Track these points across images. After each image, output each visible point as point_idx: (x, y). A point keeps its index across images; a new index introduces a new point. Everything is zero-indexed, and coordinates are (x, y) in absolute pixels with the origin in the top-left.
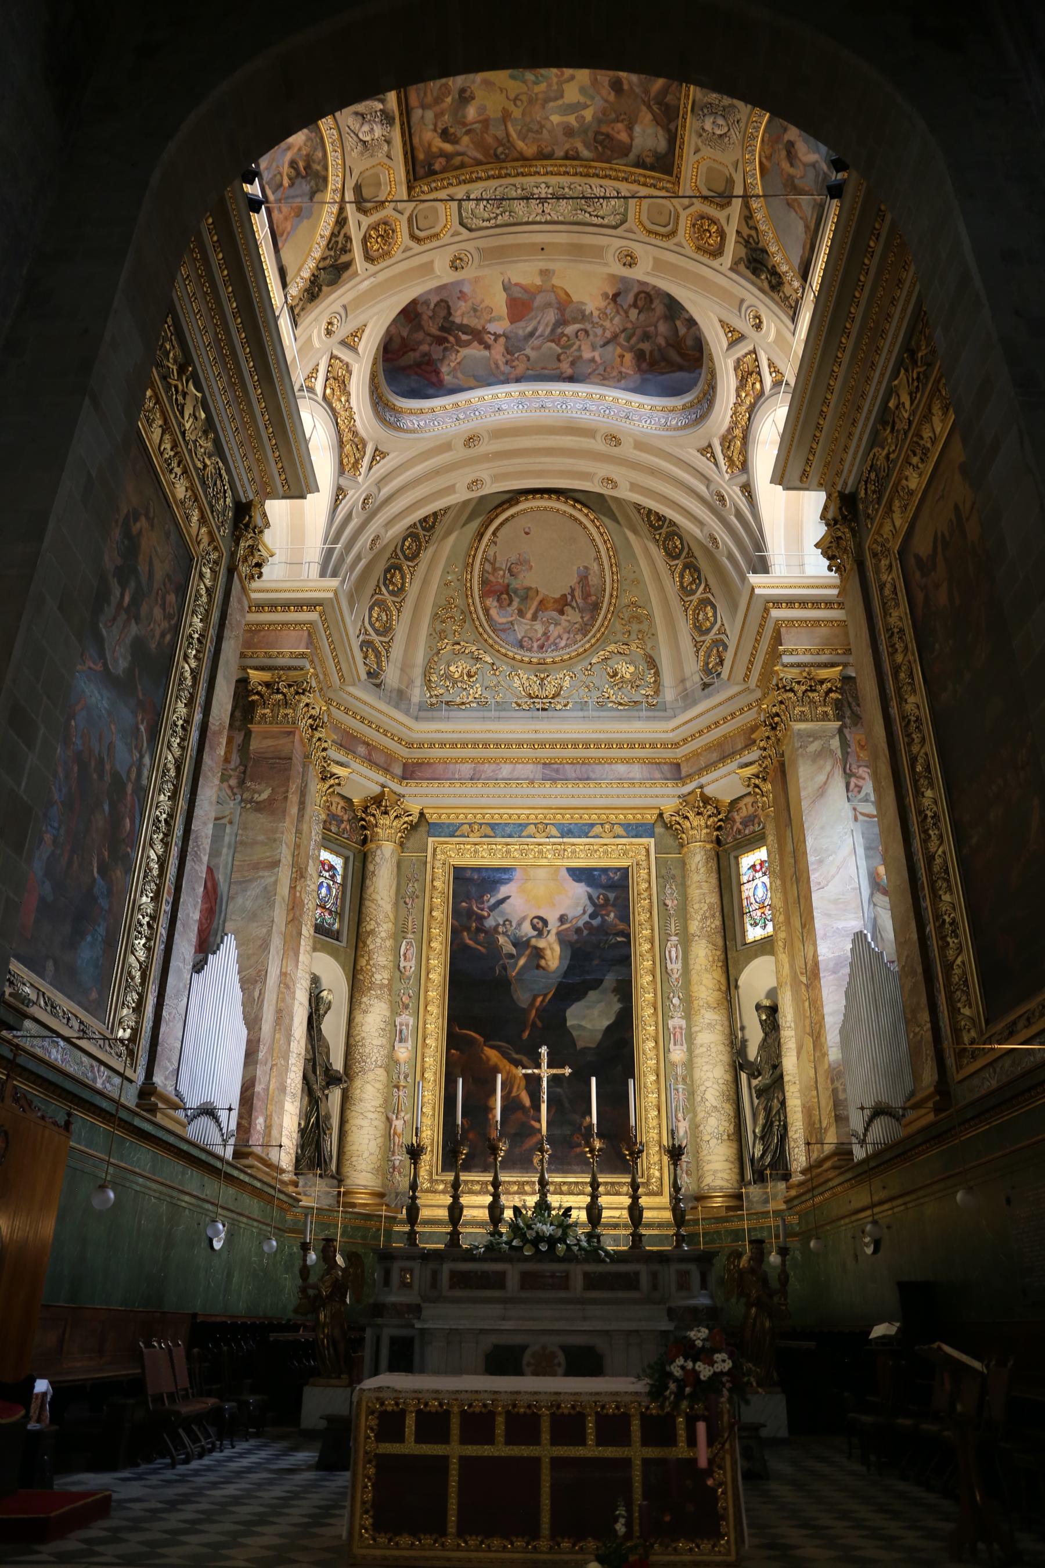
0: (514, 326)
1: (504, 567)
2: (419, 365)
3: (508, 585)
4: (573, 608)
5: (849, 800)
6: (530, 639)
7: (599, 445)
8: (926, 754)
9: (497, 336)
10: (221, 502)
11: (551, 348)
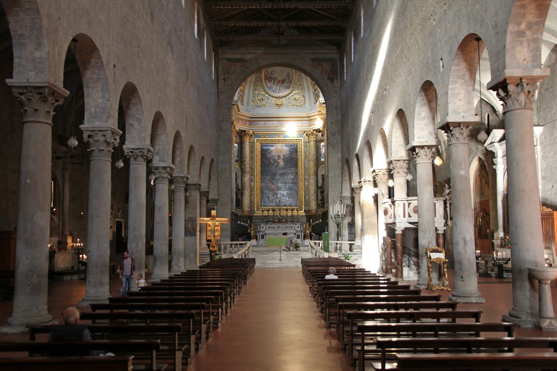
3: (271, 77)
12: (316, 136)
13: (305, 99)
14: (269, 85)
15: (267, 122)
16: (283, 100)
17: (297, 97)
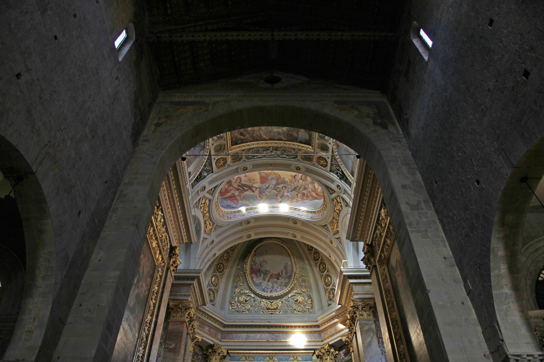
0: (262, 185)
1: (258, 263)
2: (231, 197)
3: (259, 270)
4: (282, 277)
5: (379, 347)
6: (267, 288)
7: (291, 224)
8: (400, 332)
9: (256, 188)
10: (166, 247)
11: (274, 192)
12: (335, 357)
13: (312, 301)
14: (257, 281)
15: (251, 335)
16: (279, 302)
17: (300, 298)
